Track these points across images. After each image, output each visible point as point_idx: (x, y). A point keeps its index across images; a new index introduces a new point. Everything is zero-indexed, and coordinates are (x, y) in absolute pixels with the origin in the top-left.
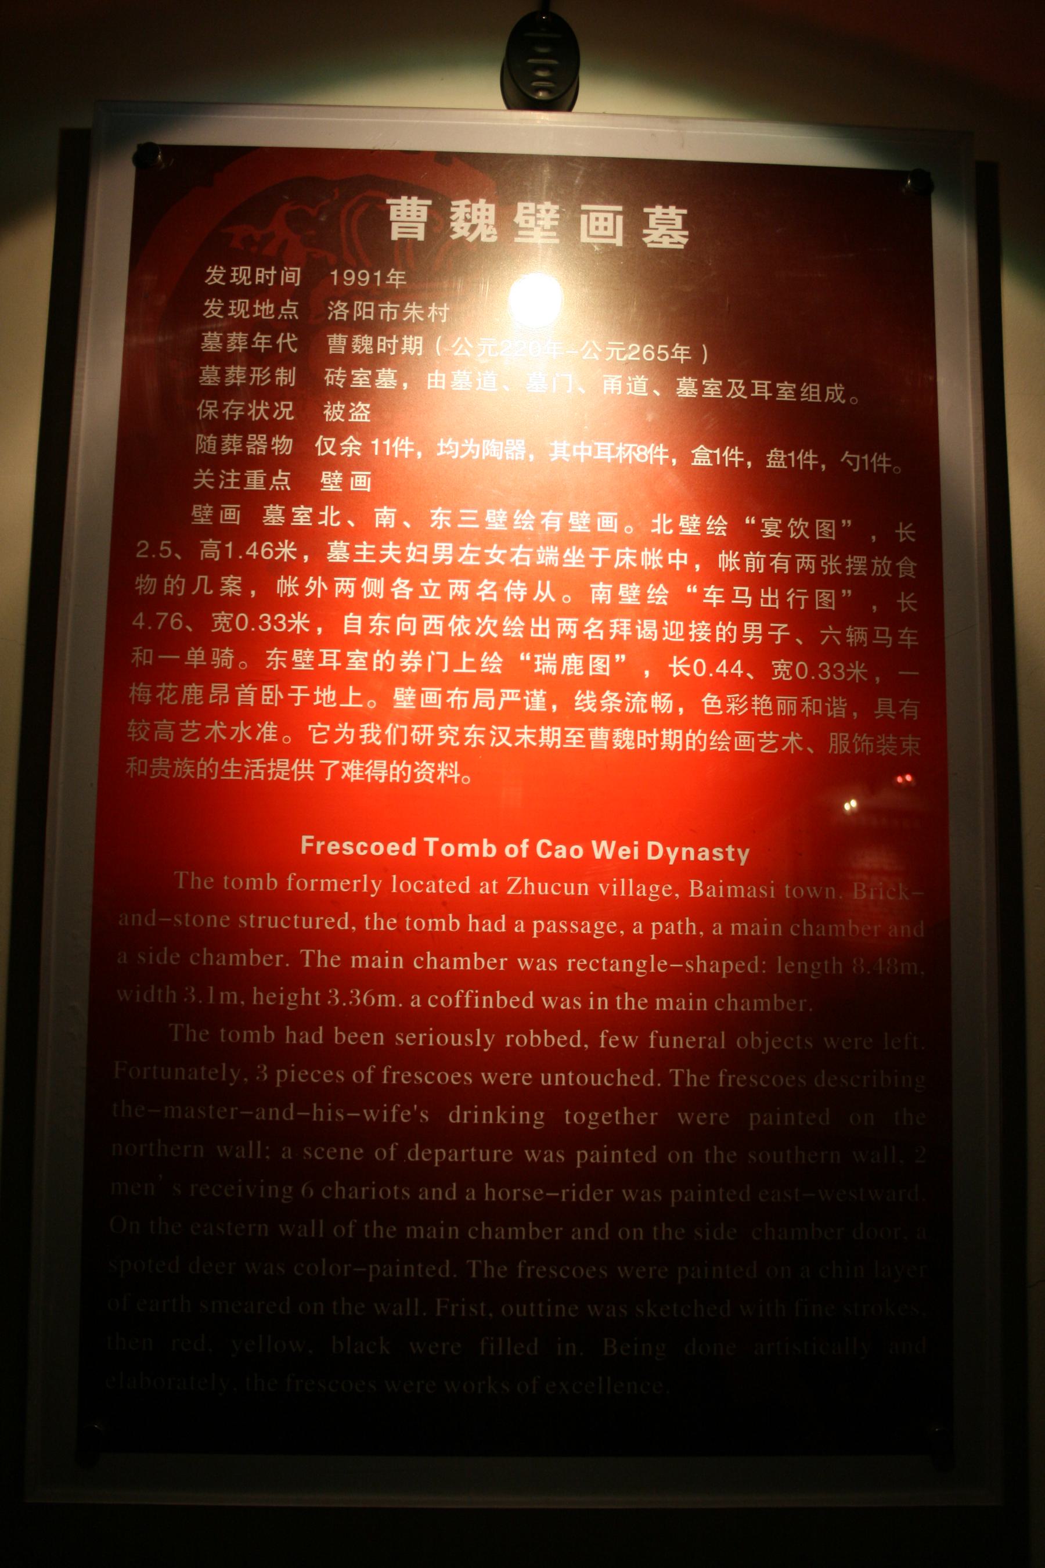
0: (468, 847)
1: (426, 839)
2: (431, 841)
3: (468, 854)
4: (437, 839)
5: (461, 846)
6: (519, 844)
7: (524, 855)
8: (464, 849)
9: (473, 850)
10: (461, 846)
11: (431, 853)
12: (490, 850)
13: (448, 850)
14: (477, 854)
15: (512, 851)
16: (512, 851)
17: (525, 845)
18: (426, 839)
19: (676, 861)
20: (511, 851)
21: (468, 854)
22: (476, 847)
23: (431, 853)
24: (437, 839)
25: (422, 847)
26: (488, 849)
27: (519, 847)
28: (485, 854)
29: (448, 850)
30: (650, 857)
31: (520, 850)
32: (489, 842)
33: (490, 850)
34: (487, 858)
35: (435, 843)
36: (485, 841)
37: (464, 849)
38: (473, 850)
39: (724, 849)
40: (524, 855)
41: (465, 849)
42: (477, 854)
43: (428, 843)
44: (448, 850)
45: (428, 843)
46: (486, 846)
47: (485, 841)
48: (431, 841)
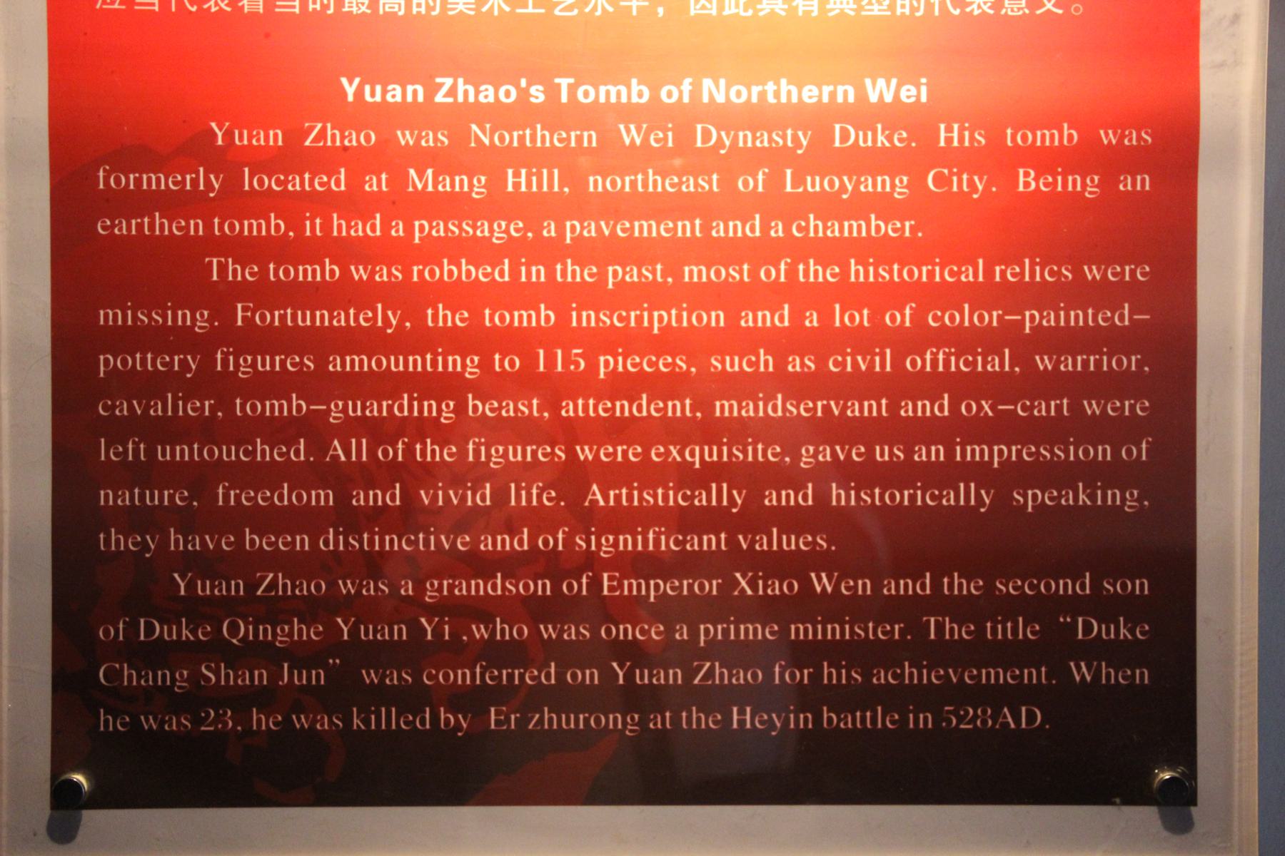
0: (613, 90)
1: (557, 80)
2: (564, 82)
3: (613, 100)
4: (572, 81)
5: (603, 89)
6: (678, 84)
7: (686, 99)
8: (608, 93)
9: (619, 94)
10: (603, 89)
11: (564, 99)
12: (640, 95)
13: (586, 94)
15: (670, 95)
16: (670, 95)
17: (686, 86)
18: (557, 80)
21: (613, 100)
22: (623, 89)
23: (564, 99)
24: (572, 81)
25: (552, 91)
26: (638, 93)
27: (678, 88)
28: (635, 99)
29: (586, 94)
31: (681, 92)
32: (639, 84)
33: (640, 95)
34: (638, 104)
35: (569, 86)
36: (634, 81)
37: (608, 93)
38: (619, 94)
40: (686, 99)
41: (610, 93)
42: (624, 99)
43: (559, 85)
44: (586, 94)
45: (559, 85)
47: (634, 81)
48: (564, 82)
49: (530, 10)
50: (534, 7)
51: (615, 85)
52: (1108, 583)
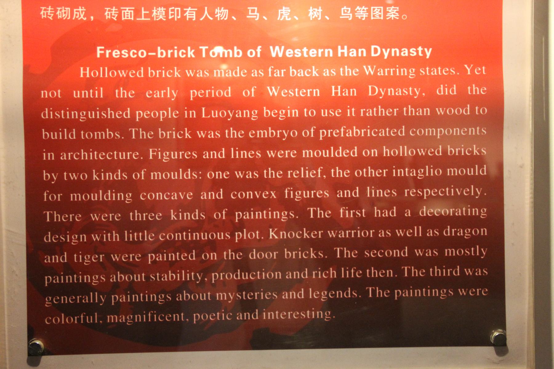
3: (226, 56)
12: (238, 53)
14: (231, 56)
15: (251, 53)
16: (251, 53)
19: (388, 57)
20: (251, 53)
22: (230, 51)
28: (236, 56)
30: (373, 55)
32: (238, 48)
33: (238, 53)
34: (237, 58)
36: (235, 48)
38: (228, 53)
39: (416, 49)
46: (236, 50)
47: (235, 48)
49: (143, 19)
50: (145, 18)
51: (227, 50)
52: (367, 252)
